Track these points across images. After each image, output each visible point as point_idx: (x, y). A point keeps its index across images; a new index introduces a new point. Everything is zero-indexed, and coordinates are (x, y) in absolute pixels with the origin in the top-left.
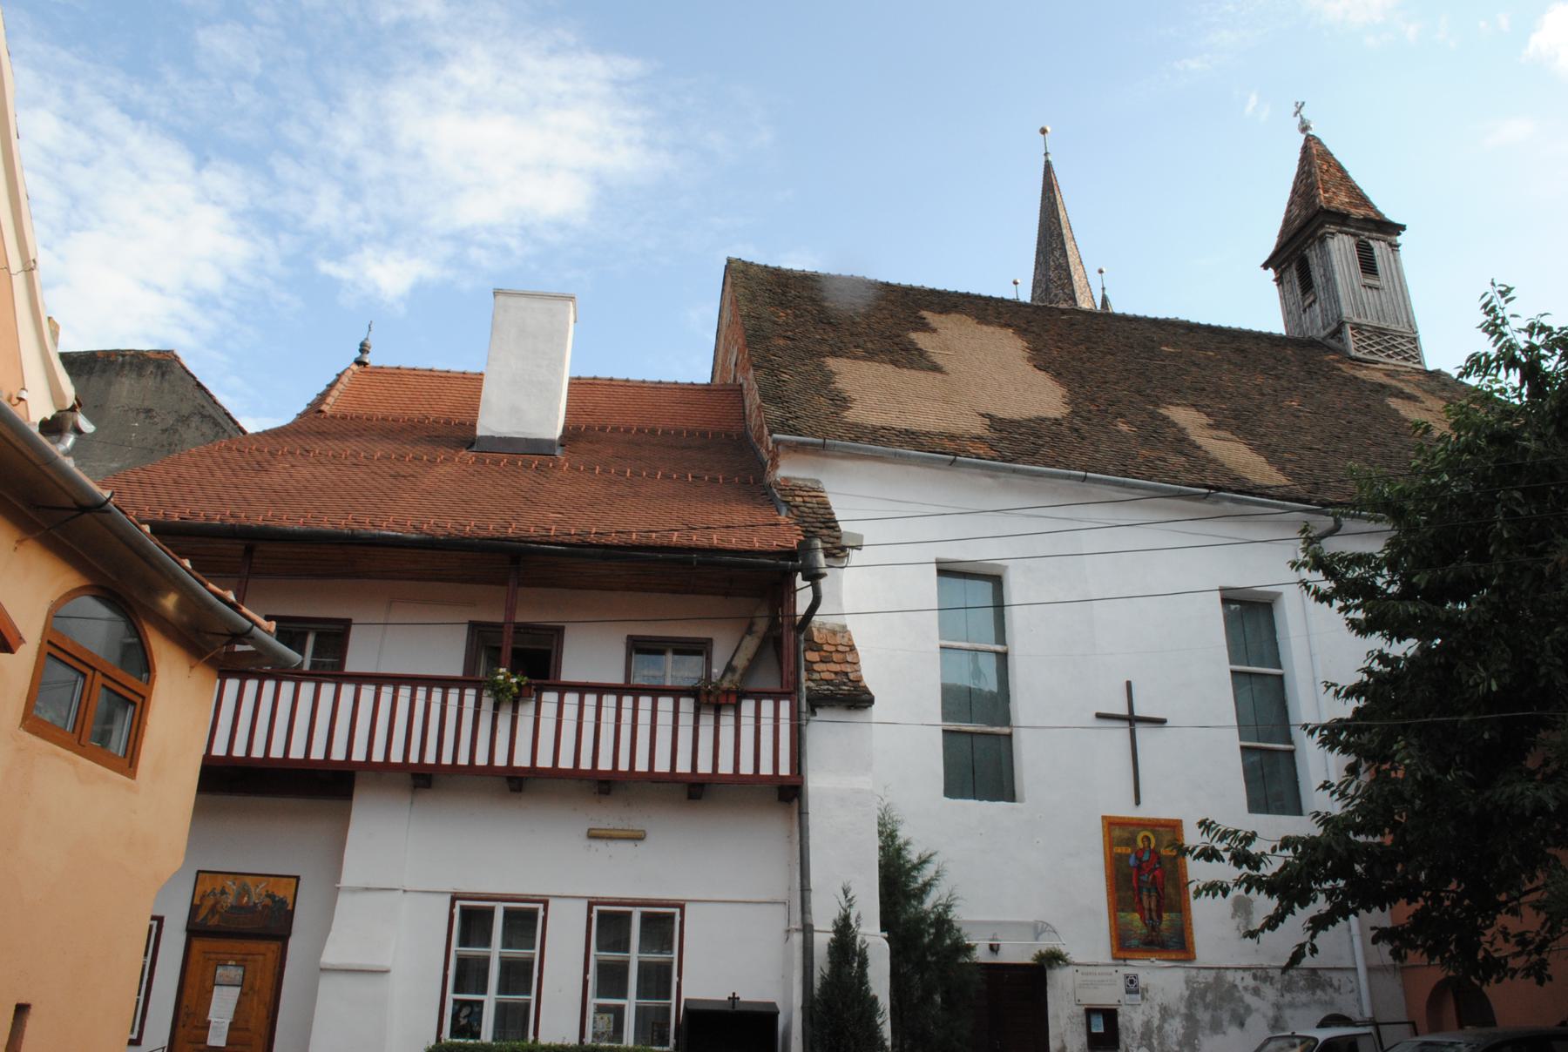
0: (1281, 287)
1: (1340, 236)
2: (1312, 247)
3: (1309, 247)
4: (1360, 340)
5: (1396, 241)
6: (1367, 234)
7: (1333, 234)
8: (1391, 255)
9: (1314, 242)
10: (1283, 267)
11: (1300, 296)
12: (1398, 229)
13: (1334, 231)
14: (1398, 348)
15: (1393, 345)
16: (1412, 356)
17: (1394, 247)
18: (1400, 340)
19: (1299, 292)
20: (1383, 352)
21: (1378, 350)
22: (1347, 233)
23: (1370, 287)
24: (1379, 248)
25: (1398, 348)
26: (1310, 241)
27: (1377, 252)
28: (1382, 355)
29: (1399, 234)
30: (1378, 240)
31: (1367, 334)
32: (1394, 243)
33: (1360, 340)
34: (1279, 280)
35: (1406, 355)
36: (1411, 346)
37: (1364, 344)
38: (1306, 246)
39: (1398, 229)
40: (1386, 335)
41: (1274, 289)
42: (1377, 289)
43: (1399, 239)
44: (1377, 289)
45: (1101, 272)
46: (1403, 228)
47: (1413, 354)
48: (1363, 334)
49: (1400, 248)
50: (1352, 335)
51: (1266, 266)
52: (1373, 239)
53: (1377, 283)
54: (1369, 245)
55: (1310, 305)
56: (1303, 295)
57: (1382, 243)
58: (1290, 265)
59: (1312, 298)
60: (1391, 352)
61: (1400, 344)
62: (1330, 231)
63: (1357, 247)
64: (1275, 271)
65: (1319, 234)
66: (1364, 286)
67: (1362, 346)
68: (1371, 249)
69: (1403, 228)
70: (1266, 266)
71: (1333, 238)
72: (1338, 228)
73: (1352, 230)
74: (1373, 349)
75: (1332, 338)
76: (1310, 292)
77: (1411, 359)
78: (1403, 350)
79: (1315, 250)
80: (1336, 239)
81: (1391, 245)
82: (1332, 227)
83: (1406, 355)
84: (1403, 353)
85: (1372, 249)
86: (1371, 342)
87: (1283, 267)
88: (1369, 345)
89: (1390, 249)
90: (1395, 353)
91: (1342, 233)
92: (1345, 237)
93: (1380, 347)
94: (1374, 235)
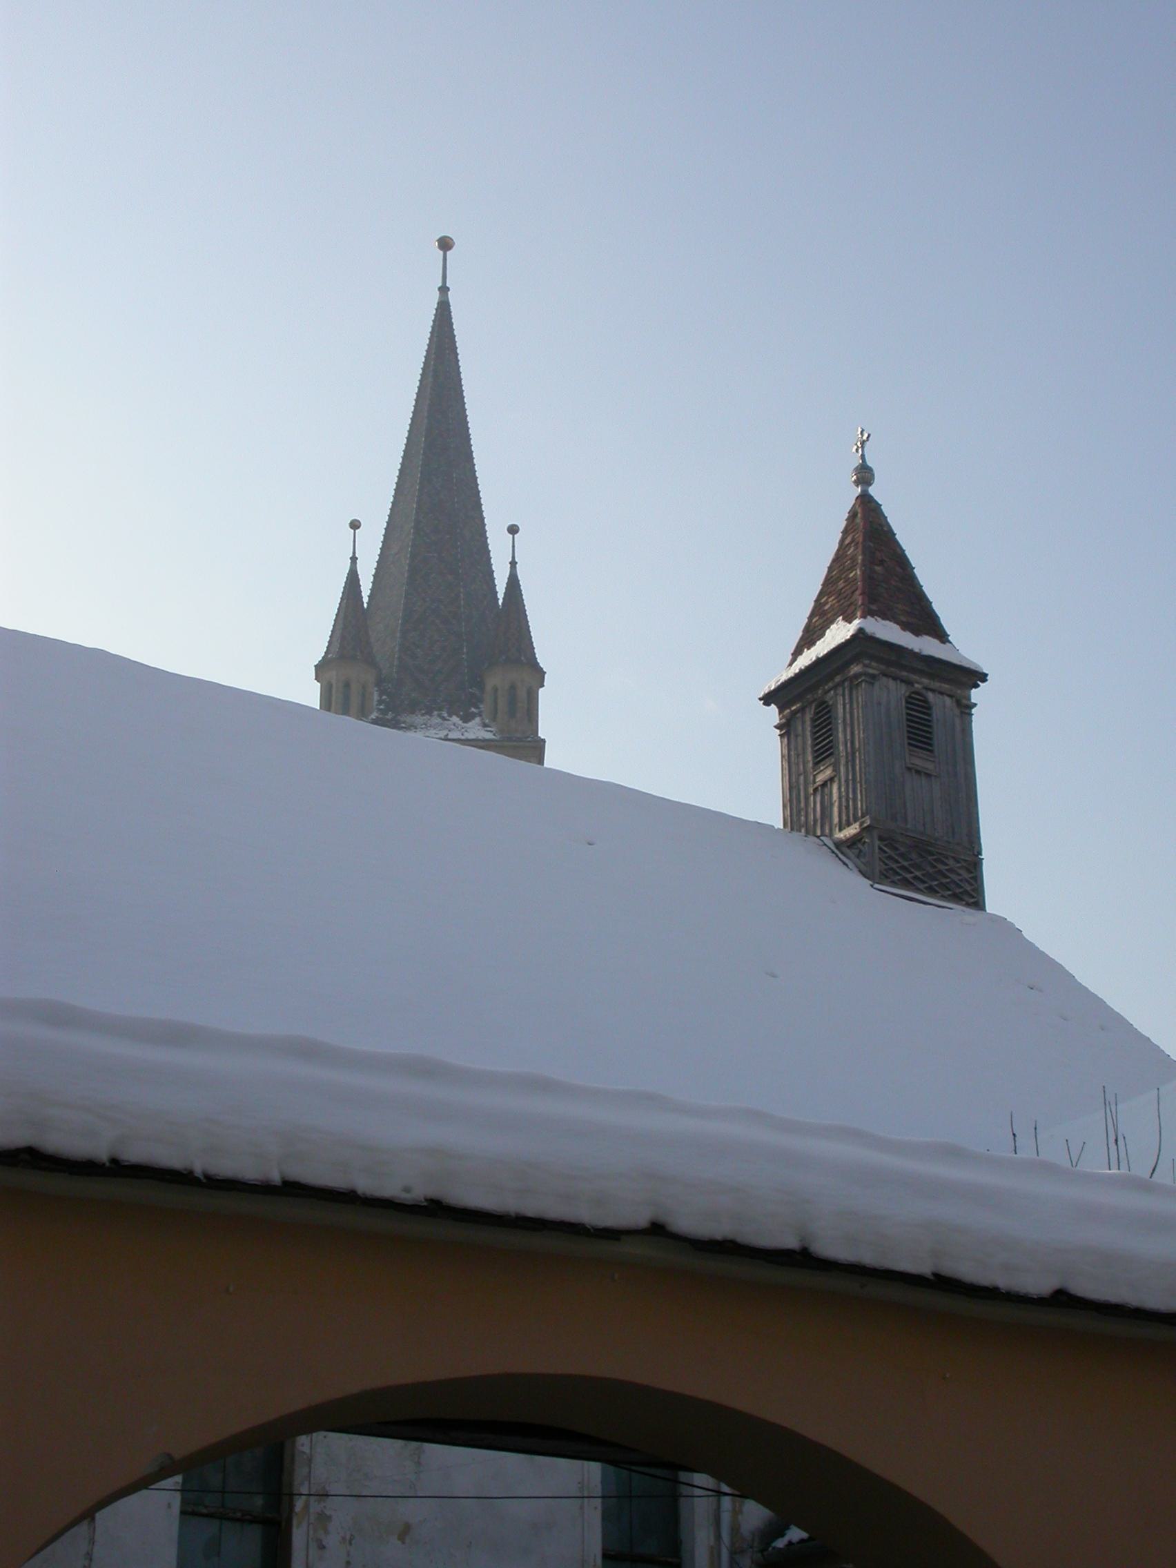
0: (786, 740)
1: (884, 679)
2: (840, 691)
3: (835, 688)
4: (890, 858)
5: (969, 699)
6: (926, 681)
7: (873, 677)
8: (957, 721)
9: (843, 682)
10: (794, 708)
11: (810, 765)
12: (976, 677)
13: (875, 672)
14: (947, 877)
15: (940, 872)
16: (966, 892)
17: (966, 708)
18: (951, 862)
19: (810, 758)
20: (924, 882)
21: (916, 878)
22: (895, 679)
23: (918, 772)
24: (941, 705)
25: (947, 877)
26: (838, 679)
27: (937, 713)
28: (921, 886)
29: (978, 686)
30: (941, 693)
31: (902, 850)
32: (964, 702)
33: (890, 858)
34: (786, 728)
35: (958, 891)
36: (966, 875)
37: (894, 866)
38: (831, 684)
39: (976, 677)
40: (931, 854)
41: (772, 745)
42: (928, 775)
43: (975, 695)
44: (928, 775)
45: (513, 530)
46: (983, 677)
47: (969, 888)
48: (896, 849)
49: (973, 711)
50: (880, 848)
51: (768, 699)
52: (933, 691)
53: (930, 766)
54: (926, 701)
55: (824, 785)
56: (816, 764)
57: (948, 701)
58: (802, 710)
59: (828, 772)
60: (936, 883)
61: (951, 870)
62: (871, 671)
63: (907, 702)
64: (780, 712)
65: (852, 673)
66: (909, 769)
67: (892, 869)
68: (926, 707)
69: (983, 677)
70: (768, 699)
71: (872, 684)
72: (883, 667)
73: (904, 674)
74: (908, 876)
75: (849, 847)
76: (828, 761)
77: (966, 898)
78: (953, 882)
79: (844, 696)
80: (877, 684)
81: (958, 703)
82: (874, 664)
83: (958, 891)
84: (953, 886)
85: (929, 708)
86: (906, 864)
87: (794, 708)
88: (903, 868)
89: (957, 711)
90: (942, 885)
91: (885, 675)
92: (891, 683)
93: (918, 874)
94: (936, 685)
